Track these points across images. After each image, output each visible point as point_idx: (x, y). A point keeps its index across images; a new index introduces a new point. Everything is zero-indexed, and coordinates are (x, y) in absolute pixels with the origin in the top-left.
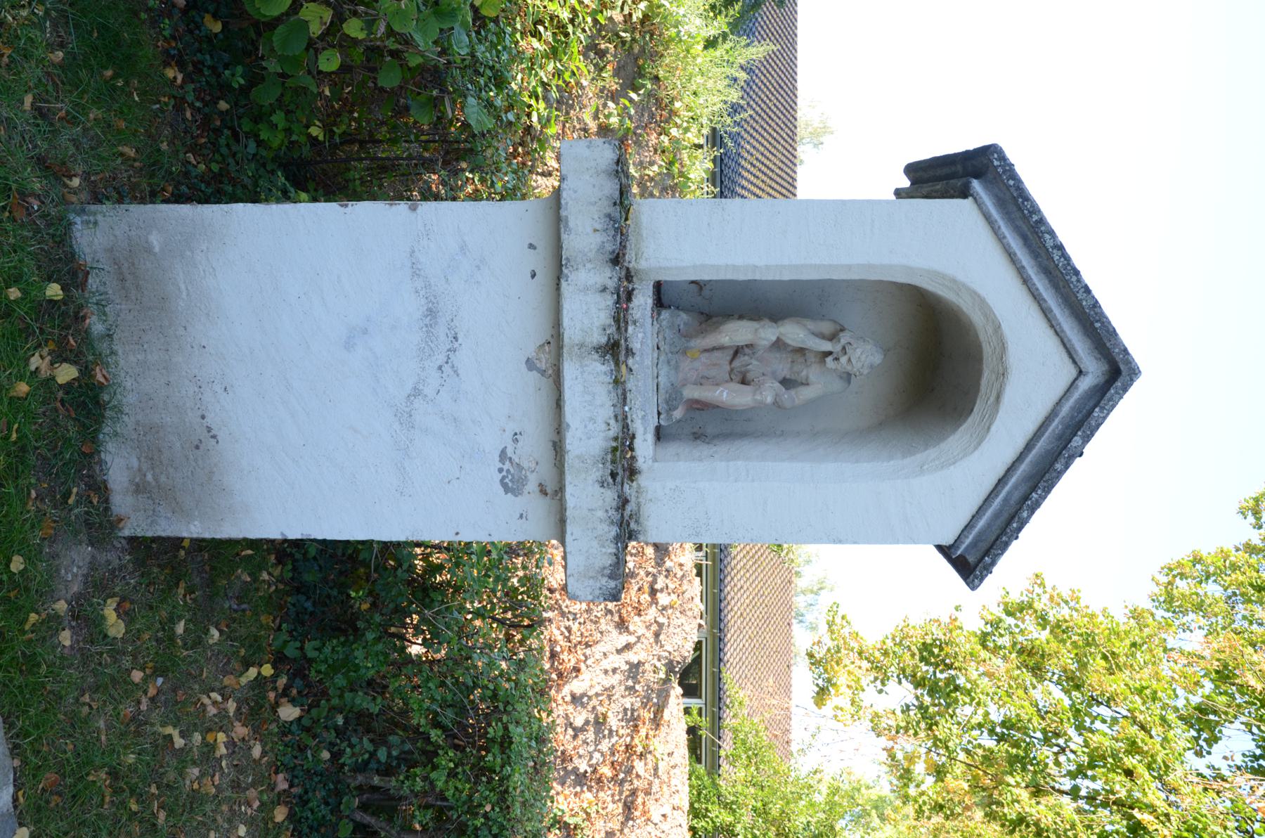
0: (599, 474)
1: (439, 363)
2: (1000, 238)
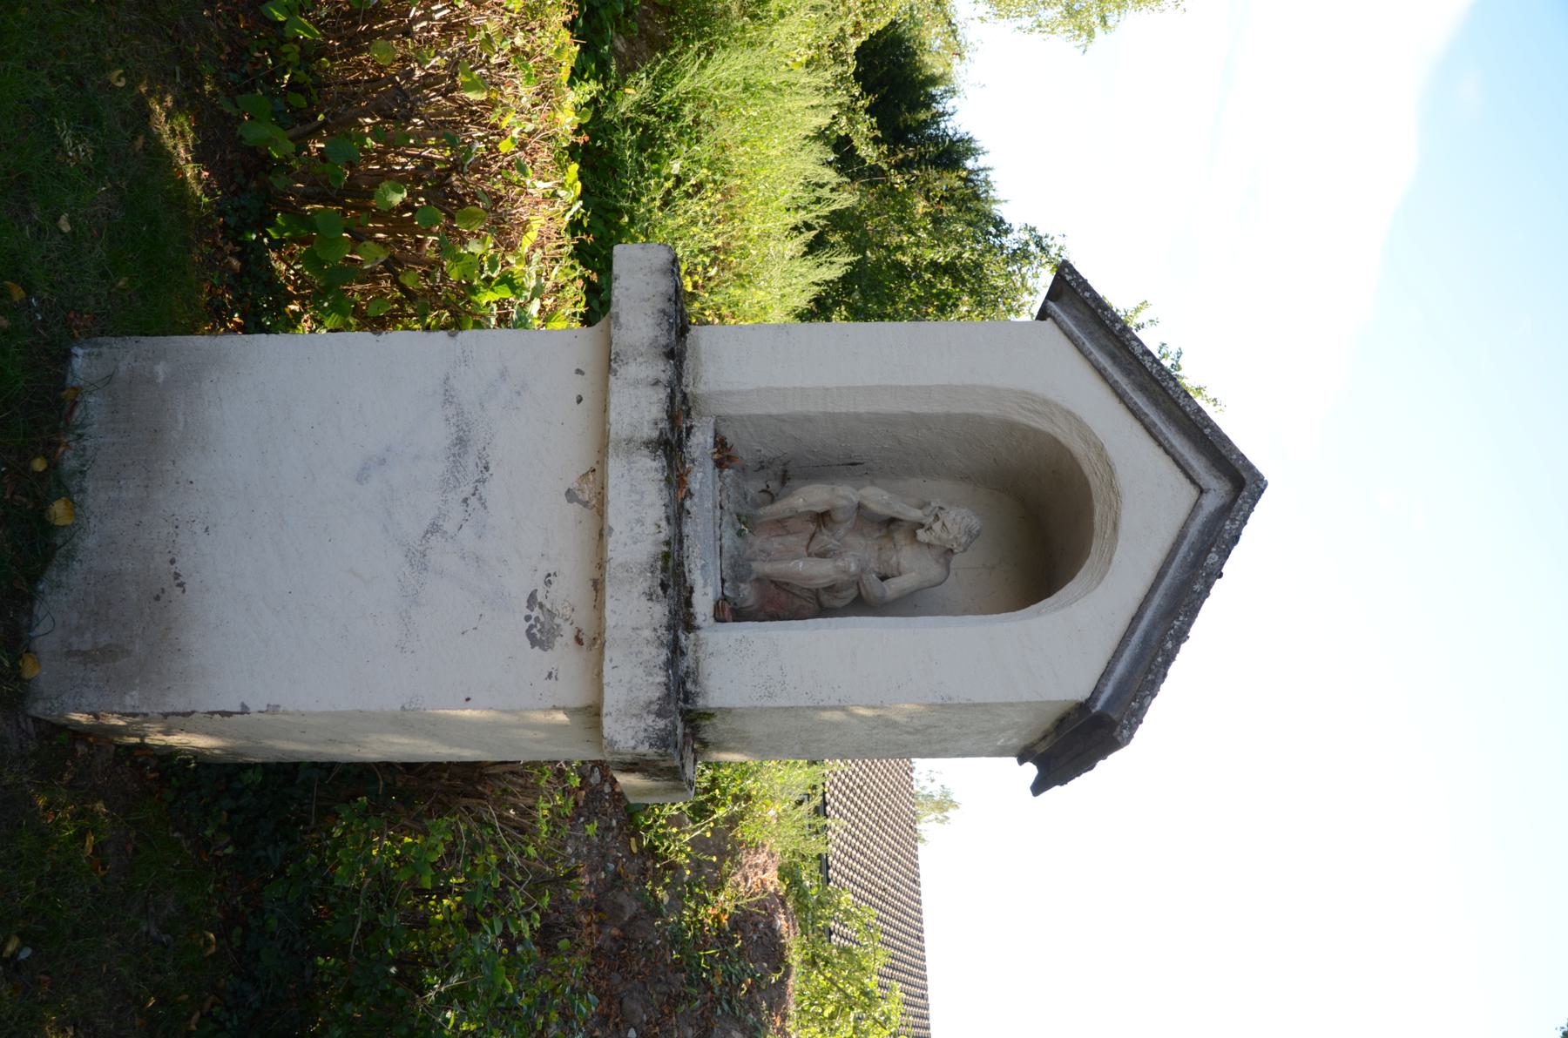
0: (646, 585)
1: (465, 495)
2: (1086, 355)
